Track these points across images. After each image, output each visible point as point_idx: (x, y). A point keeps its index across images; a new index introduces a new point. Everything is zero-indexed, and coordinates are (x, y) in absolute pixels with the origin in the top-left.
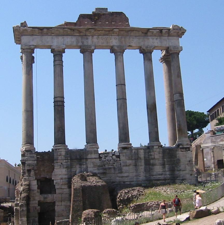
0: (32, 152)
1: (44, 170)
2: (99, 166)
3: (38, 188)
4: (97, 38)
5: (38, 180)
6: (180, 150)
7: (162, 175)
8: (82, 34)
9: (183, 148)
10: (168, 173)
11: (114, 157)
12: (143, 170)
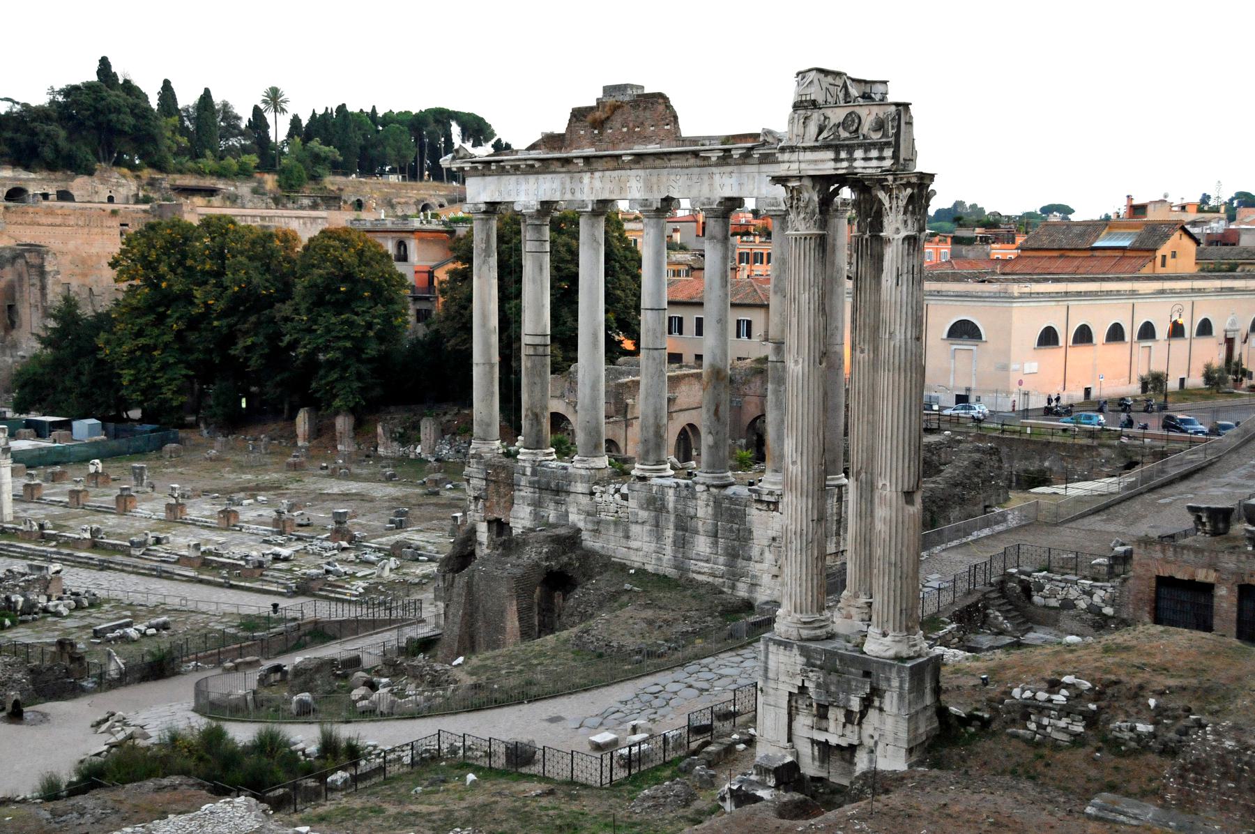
0: (481, 457)
1: (498, 503)
2: (588, 514)
3: (491, 540)
4: (602, 178)
5: (489, 522)
6: (755, 505)
7: (707, 561)
8: (571, 167)
9: (760, 501)
10: (722, 559)
11: (617, 496)
12: (670, 540)
